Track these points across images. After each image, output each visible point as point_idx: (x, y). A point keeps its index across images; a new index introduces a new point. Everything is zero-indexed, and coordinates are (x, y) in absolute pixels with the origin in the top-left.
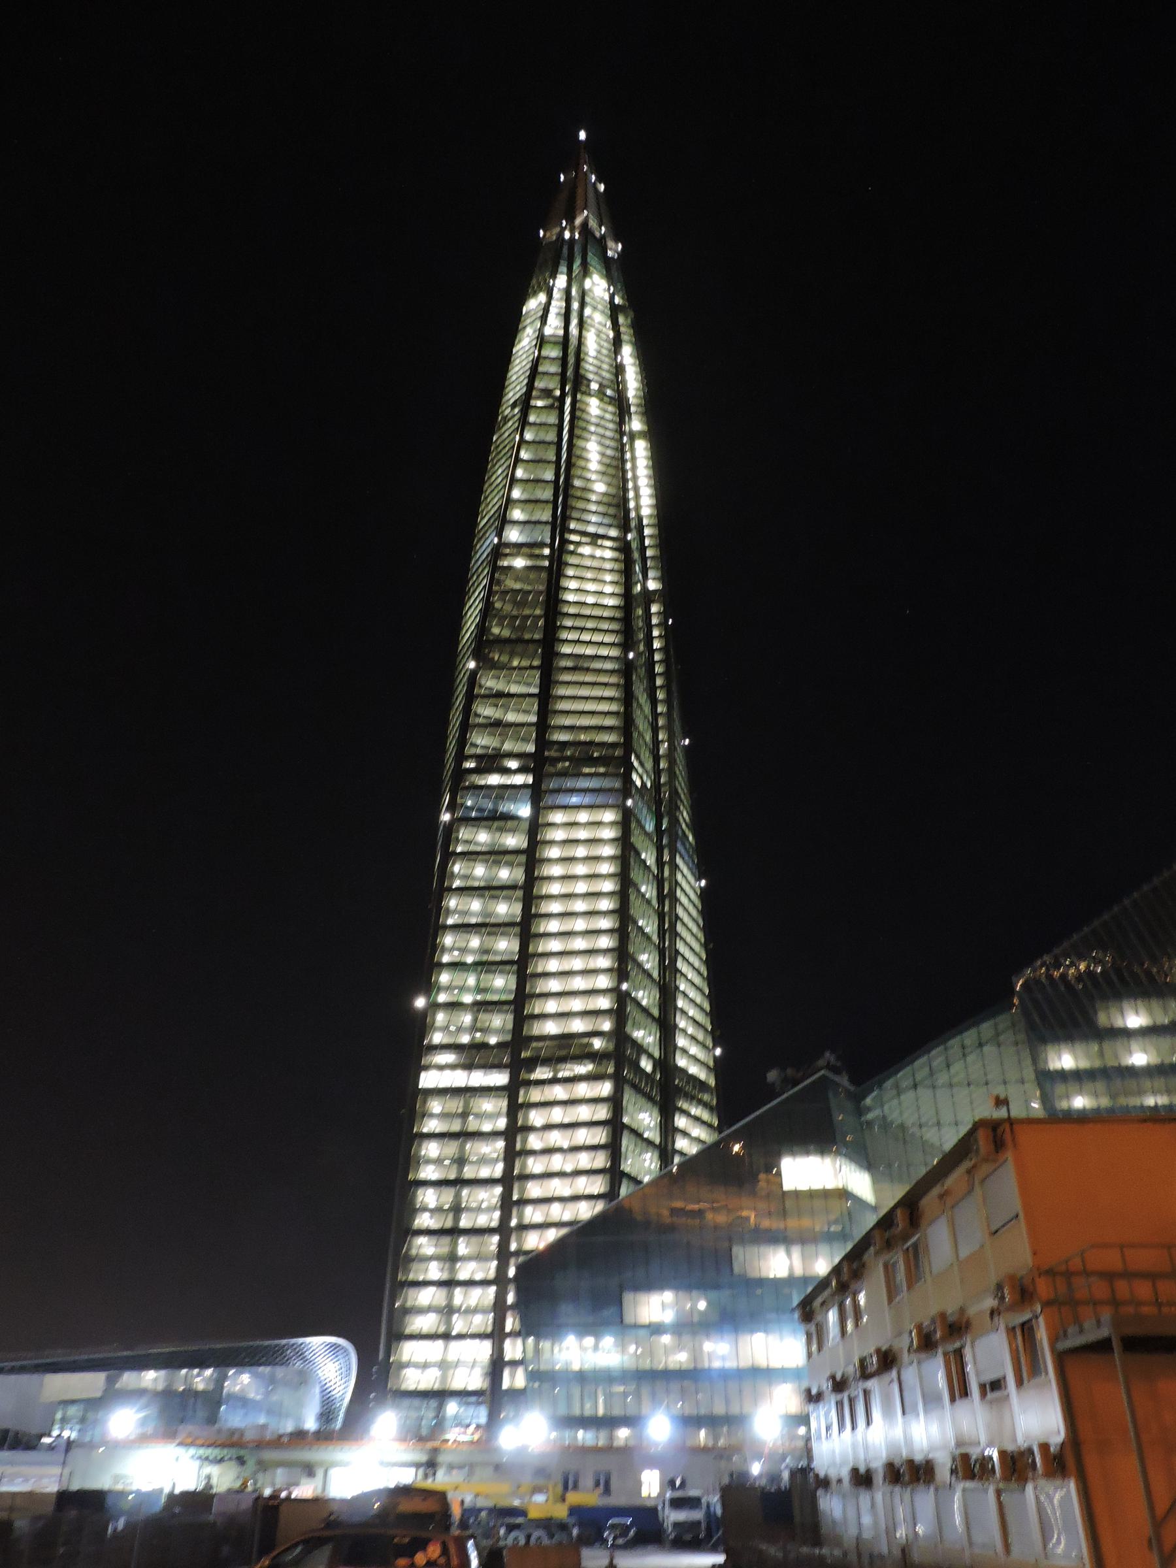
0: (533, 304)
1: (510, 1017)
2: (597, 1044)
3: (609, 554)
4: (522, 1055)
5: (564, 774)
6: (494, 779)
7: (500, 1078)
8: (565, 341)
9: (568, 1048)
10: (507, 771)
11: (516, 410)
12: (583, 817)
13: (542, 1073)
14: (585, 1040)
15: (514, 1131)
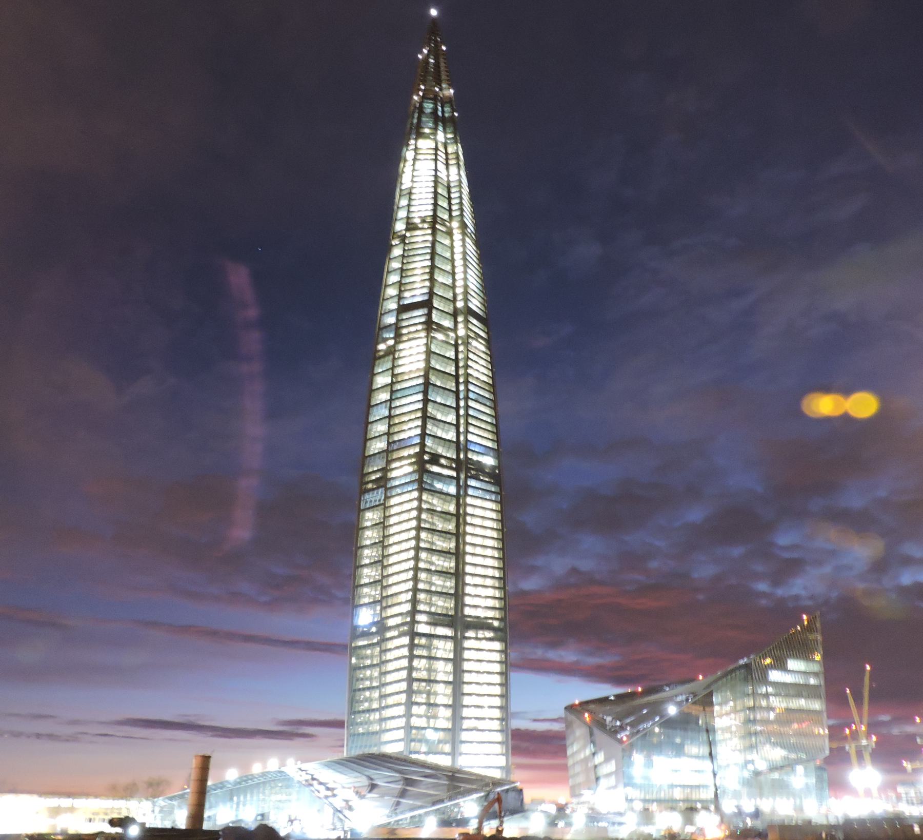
0: (425, 144)
1: (453, 602)
2: (496, 624)
3: (483, 348)
4: (458, 623)
5: (476, 478)
6: (435, 469)
7: (448, 632)
8: (449, 188)
9: (480, 624)
10: (442, 466)
11: (426, 226)
12: (478, 502)
13: (470, 634)
14: (490, 621)
15: (457, 661)
